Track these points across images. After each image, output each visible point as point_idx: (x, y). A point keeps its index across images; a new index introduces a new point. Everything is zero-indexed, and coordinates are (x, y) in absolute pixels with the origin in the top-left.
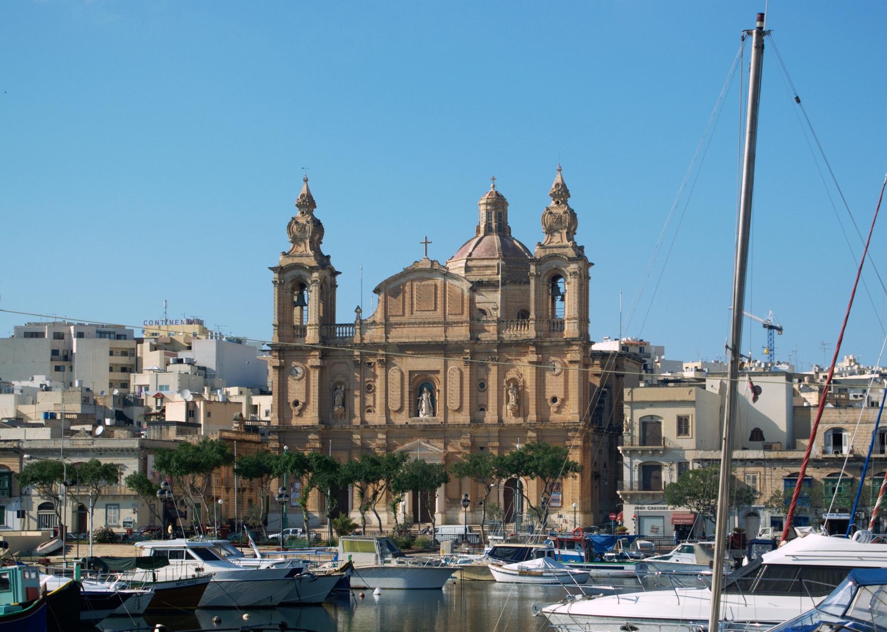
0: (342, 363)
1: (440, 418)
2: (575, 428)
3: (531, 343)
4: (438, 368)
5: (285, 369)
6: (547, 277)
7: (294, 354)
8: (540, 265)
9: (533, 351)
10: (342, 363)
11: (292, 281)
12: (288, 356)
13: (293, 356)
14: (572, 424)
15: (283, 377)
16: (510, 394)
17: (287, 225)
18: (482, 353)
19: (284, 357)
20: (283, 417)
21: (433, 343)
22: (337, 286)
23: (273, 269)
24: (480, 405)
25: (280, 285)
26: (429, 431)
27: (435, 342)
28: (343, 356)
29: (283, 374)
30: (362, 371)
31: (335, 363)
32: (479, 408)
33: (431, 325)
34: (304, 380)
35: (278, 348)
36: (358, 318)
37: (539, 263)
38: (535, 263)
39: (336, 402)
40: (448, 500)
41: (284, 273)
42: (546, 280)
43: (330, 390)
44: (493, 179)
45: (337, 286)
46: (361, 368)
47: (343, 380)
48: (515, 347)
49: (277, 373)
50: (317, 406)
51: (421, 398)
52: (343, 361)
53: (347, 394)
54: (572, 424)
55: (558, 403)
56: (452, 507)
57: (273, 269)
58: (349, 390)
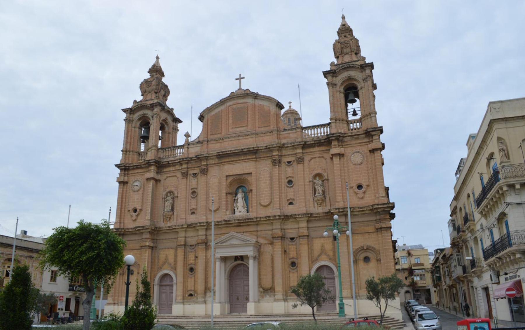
0: (173, 176)
1: (252, 215)
2: (384, 211)
3: (333, 138)
4: (250, 171)
5: (128, 184)
6: (343, 87)
7: (136, 171)
8: (336, 77)
9: (335, 145)
10: (173, 176)
11: (139, 119)
12: (132, 174)
13: (135, 173)
14: (382, 206)
15: (126, 191)
16: (316, 187)
17: (140, 83)
18: (289, 155)
19: (128, 174)
20: (124, 223)
21: (246, 150)
22: (178, 130)
23: (125, 111)
24: (288, 200)
25: (128, 121)
26: (243, 226)
27: (247, 149)
28: (173, 171)
29: (126, 188)
30: (188, 181)
31: (168, 177)
32: (288, 203)
33: (244, 138)
34: (141, 192)
35: (123, 167)
36: (187, 141)
37: (335, 75)
38: (331, 74)
39: (166, 207)
40: (261, 290)
41: (134, 114)
42: (342, 90)
43: (163, 199)
44: (290, 103)
45: (178, 130)
46: (187, 178)
47: (173, 189)
48: (319, 146)
49: (122, 187)
50: (150, 211)
51: (236, 198)
52: (174, 175)
53: (176, 201)
54: (382, 206)
55: (363, 190)
56: (266, 295)
57: (125, 111)
58: (177, 197)
